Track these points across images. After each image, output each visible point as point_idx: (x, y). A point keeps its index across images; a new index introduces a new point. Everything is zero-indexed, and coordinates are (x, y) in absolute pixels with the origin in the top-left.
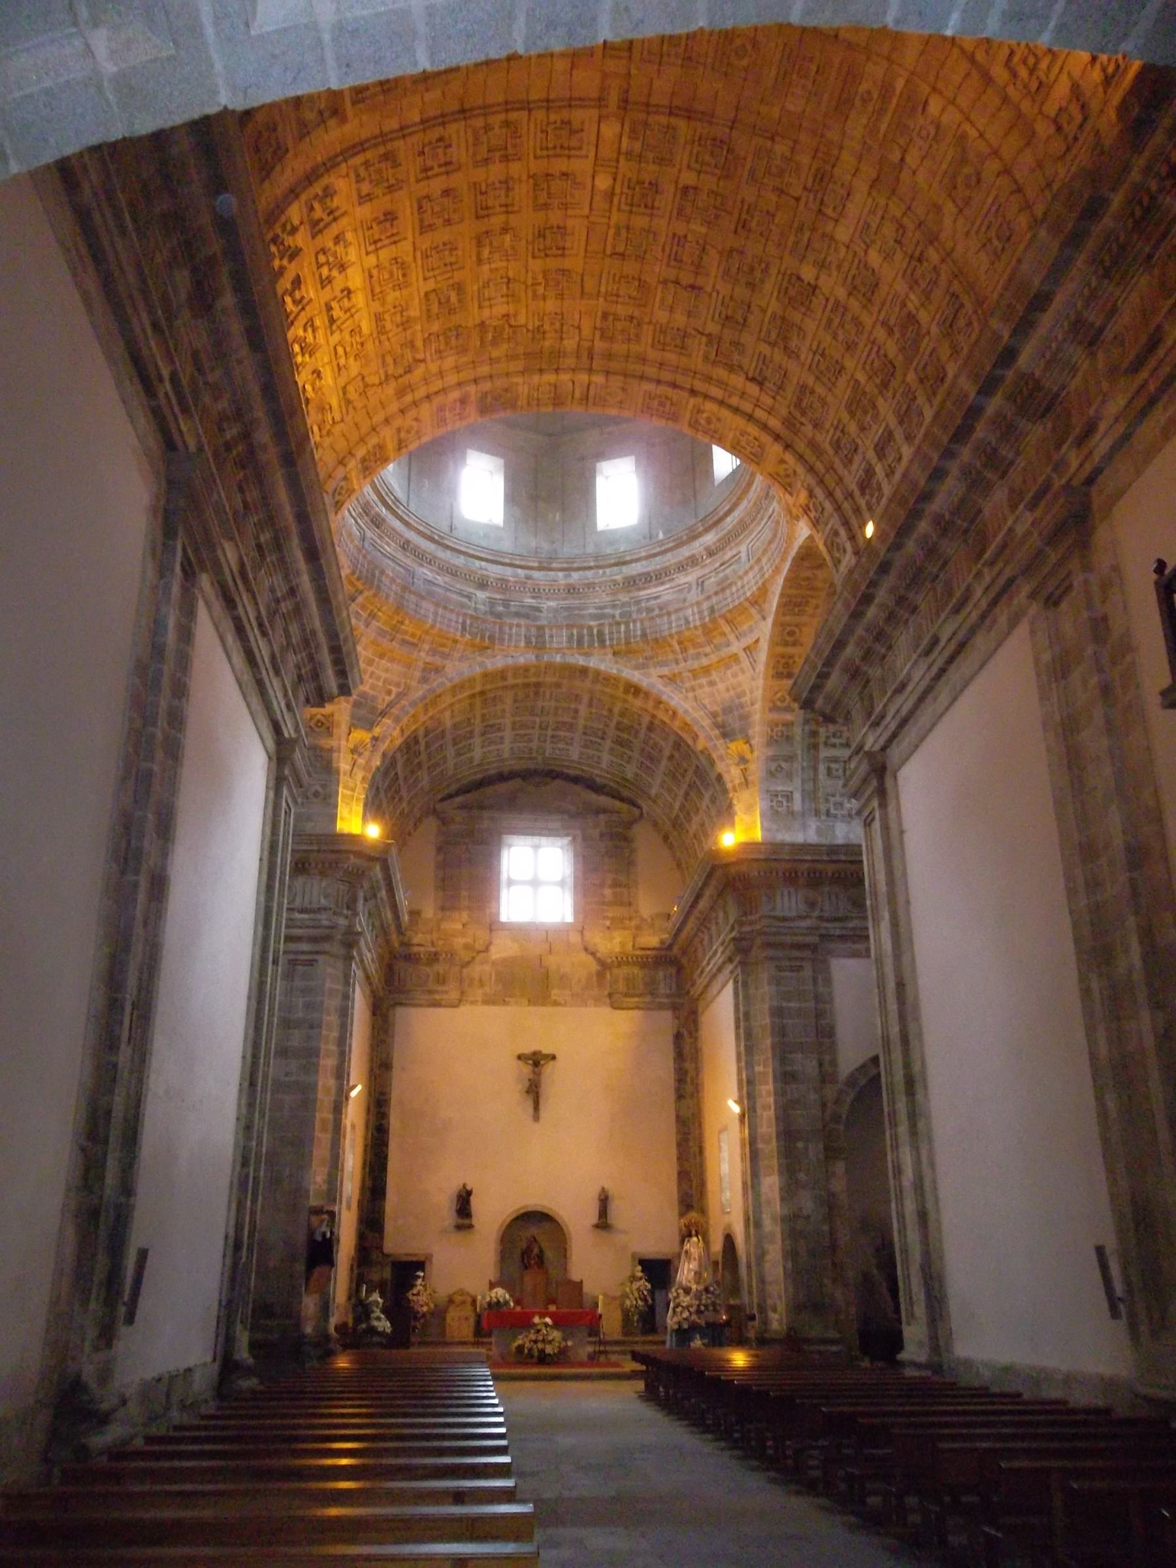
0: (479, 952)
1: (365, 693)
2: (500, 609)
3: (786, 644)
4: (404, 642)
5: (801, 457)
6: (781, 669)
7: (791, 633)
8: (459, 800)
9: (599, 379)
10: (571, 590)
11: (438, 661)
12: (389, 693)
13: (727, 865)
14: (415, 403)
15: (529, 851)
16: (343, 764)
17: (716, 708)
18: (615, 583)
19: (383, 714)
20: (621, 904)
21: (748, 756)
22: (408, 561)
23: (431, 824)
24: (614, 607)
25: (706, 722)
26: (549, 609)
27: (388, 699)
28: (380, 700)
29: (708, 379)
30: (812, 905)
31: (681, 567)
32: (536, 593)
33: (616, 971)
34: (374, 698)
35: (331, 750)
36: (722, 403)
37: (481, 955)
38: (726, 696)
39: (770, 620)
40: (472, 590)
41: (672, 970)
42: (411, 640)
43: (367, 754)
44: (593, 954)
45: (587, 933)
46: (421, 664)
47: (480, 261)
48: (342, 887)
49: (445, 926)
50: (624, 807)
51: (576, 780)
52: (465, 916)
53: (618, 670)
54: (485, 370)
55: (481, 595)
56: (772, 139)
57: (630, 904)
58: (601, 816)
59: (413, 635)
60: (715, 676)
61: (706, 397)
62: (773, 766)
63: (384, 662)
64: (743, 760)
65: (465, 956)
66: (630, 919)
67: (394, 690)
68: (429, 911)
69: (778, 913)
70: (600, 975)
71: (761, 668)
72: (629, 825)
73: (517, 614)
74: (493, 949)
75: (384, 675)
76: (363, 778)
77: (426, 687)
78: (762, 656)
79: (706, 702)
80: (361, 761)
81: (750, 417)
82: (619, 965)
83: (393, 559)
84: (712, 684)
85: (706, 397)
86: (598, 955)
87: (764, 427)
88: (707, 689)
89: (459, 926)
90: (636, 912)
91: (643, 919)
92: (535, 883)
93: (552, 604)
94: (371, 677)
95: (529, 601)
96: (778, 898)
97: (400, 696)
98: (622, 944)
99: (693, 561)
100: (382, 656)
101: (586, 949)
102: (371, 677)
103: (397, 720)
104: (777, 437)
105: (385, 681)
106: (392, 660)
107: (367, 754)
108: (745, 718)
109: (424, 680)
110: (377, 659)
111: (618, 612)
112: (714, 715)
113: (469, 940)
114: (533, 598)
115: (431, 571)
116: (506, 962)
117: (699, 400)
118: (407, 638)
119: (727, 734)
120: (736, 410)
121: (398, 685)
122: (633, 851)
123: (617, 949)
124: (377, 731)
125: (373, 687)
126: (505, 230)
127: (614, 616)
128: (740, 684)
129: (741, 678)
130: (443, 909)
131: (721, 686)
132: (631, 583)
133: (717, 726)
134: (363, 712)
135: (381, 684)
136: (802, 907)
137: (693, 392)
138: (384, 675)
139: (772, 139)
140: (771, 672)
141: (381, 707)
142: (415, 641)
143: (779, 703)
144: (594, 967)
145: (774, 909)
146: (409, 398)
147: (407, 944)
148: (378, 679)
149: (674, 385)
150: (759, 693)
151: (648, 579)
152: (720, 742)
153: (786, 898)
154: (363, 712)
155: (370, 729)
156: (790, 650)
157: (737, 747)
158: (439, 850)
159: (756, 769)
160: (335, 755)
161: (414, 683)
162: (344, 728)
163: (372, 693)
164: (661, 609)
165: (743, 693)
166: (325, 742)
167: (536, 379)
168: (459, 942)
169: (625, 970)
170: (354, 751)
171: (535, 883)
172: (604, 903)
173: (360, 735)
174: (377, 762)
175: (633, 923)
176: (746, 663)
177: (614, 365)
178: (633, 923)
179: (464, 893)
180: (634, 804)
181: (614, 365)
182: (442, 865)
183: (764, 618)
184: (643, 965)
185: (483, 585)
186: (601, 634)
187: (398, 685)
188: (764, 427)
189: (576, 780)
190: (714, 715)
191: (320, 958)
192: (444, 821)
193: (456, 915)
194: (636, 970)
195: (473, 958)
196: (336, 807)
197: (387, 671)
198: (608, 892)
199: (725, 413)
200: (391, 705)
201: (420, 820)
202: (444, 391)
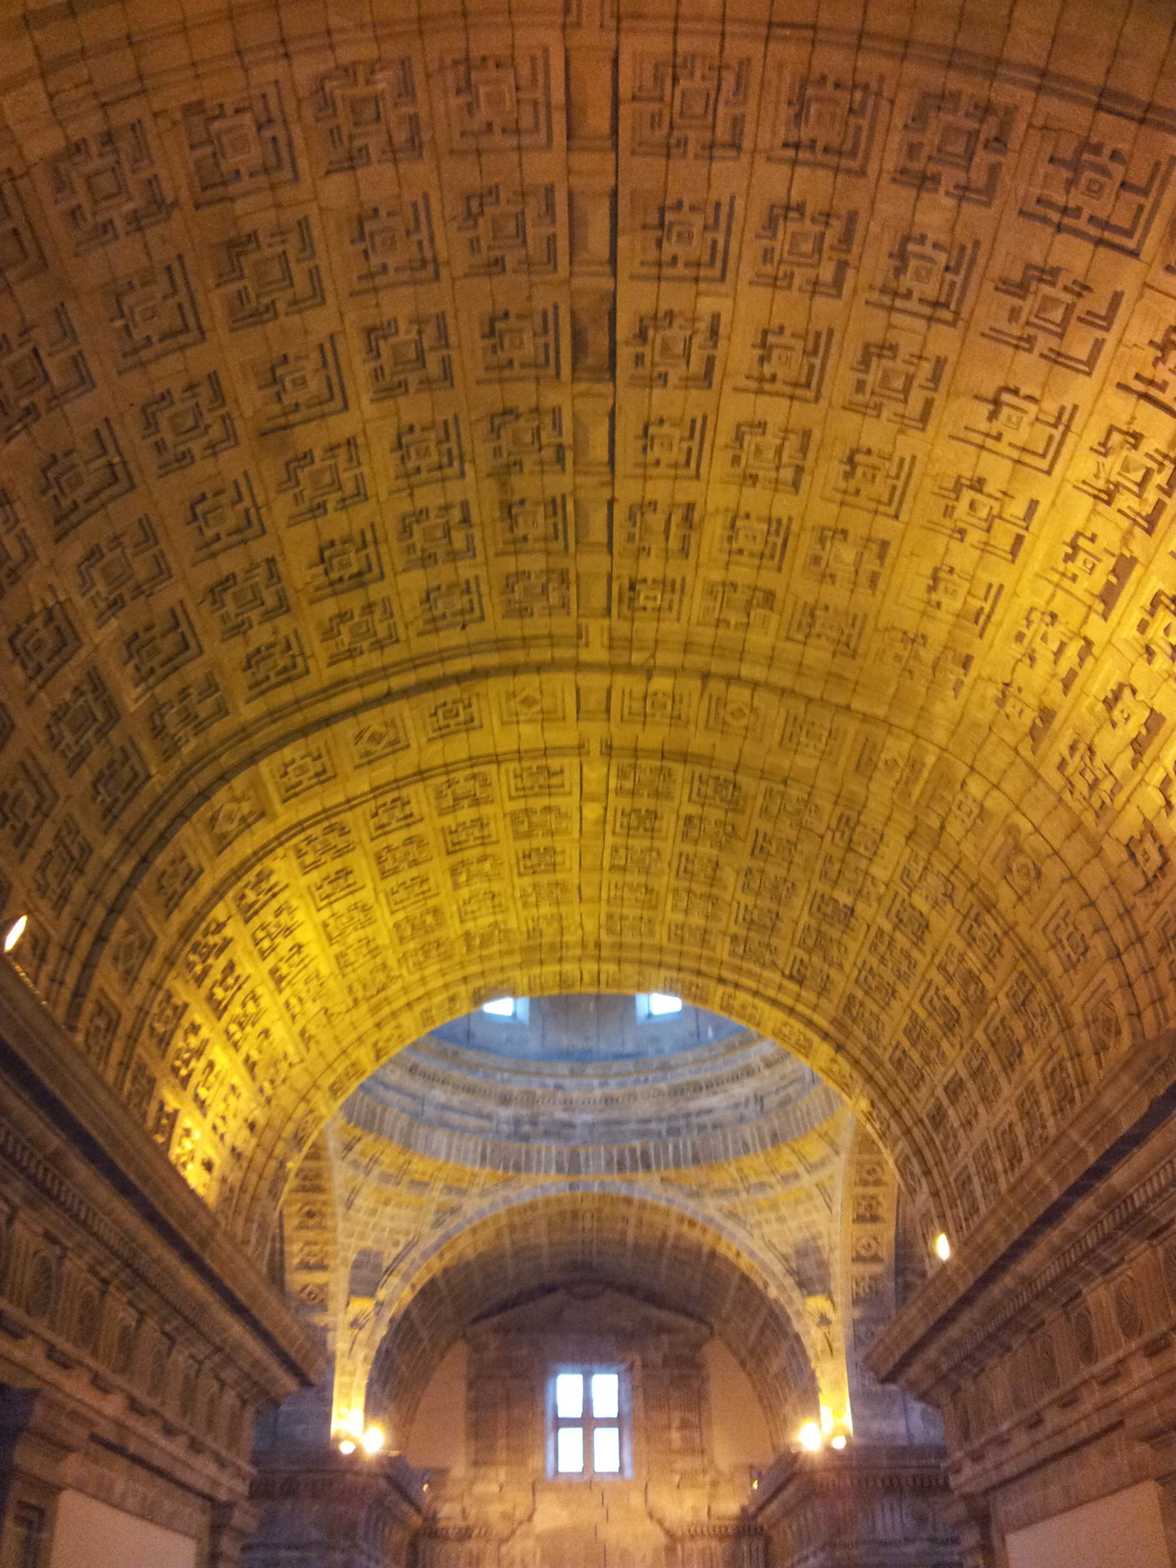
0: (520, 1523)
2: (526, 1128)
3: (865, 1183)
4: (413, 1183)
5: (856, 1063)
6: (862, 1211)
7: (871, 1172)
8: (495, 1320)
9: (610, 968)
10: (609, 1100)
11: (454, 1200)
12: (396, 1244)
13: (813, 1472)
14: (394, 1015)
15: (579, 1378)
16: (340, 1343)
17: (787, 1250)
18: (660, 1093)
19: (390, 1271)
20: (693, 1451)
21: (832, 1316)
22: (415, 1085)
23: (460, 1349)
24: (660, 1120)
25: (778, 1268)
26: (584, 1124)
27: (395, 1252)
29: (739, 970)
30: (921, 1520)
31: (735, 1078)
32: (568, 1105)
33: (689, 1545)
34: (379, 1254)
35: (325, 1329)
36: (756, 993)
37: (524, 1528)
38: (800, 1236)
39: (843, 1156)
41: (761, 1544)
43: (369, 1326)
44: (660, 1522)
45: (652, 1497)
46: (434, 1207)
47: (456, 886)
49: (480, 1488)
50: (691, 1324)
51: (631, 1290)
52: (502, 1474)
53: (669, 1201)
54: (474, 968)
55: (505, 1113)
56: (785, 782)
57: (703, 1452)
58: (664, 1337)
60: (784, 1211)
61: (737, 986)
62: (862, 1329)
63: (389, 1210)
64: (824, 1321)
65: (502, 1528)
66: (704, 1471)
67: (403, 1241)
68: (459, 1469)
69: (881, 1535)
70: (670, 1550)
71: (837, 1209)
72: (698, 1346)
73: (547, 1134)
74: (537, 1518)
75: (389, 1224)
76: (366, 1358)
77: (440, 1232)
78: (839, 1195)
79: (775, 1240)
80: (363, 1335)
81: (791, 1011)
82: (693, 1537)
83: (399, 1089)
84: (781, 1219)
85: (737, 986)
86: (667, 1524)
87: (810, 1023)
88: (775, 1226)
89: (495, 1488)
90: (711, 1461)
91: (719, 1473)
92: (587, 1422)
93: (588, 1117)
95: (560, 1115)
96: (878, 1512)
97: (410, 1246)
98: (695, 1510)
99: (749, 1072)
100: (386, 1203)
101: (651, 1516)
103: (406, 1277)
104: (826, 1036)
106: (399, 1205)
107: (369, 1326)
108: (823, 1265)
109: (437, 1224)
111: (664, 1127)
112: (785, 1258)
113: (508, 1507)
116: (555, 1537)
117: (730, 990)
119: (806, 1285)
120: (774, 1002)
122: (704, 1380)
123: (689, 1518)
124: (382, 1294)
126: (483, 859)
127: (659, 1134)
128: (814, 1222)
129: (815, 1216)
130: (476, 1464)
131: (793, 1224)
132: (677, 1092)
133: (791, 1272)
134: (364, 1273)
136: (909, 1522)
137: (721, 980)
139: (785, 782)
140: (851, 1216)
141: (386, 1264)
143: (863, 1252)
144: (662, 1539)
145: (873, 1529)
146: (386, 1011)
147: (431, 1519)
149: (699, 973)
150: (837, 1239)
151: (696, 1088)
152: (796, 1294)
153: (888, 1513)
154: (364, 1273)
155: (371, 1294)
156: (871, 1190)
157: (817, 1303)
158: (471, 1385)
159: (840, 1333)
160: (330, 1335)
161: (426, 1230)
162: (341, 1298)
163: (376, 1248)
164: (715, 1127)
165: (820, 1235)
166: (319, 1319)
167: (536, 971)
168: (494, 1511)
169: (700, 1544)
170: (355, 1324)
171: (587, 1422)
172: (672, 1452)
173: (362, 1305)
174: (383, 1331)
175: (708, 1478)
176: (820, 1201)
177: (628, 954)
178: (708, 1478)
179: (501, 1443)
180: (701, 1320)
181: (628, 954)
182: (473, 1406)
183: (837, 1153)
184: (721, 1536)
185: (505, 1100)
186: (645, 1154)
187: (407, 1233)
188: (810, 1023)
189: (631, 1290)
190: (785, 1258)
192: (477, 1348)
193: (492, 1473)
194: (714, 1544)
195: (513, 1532)
196: (329, 1402)
197: (392, 1218)
198: (675, 1436)
199: (759, 1003)
200: (399, 1259)
201: (448, 1347)
202: (428, 995)
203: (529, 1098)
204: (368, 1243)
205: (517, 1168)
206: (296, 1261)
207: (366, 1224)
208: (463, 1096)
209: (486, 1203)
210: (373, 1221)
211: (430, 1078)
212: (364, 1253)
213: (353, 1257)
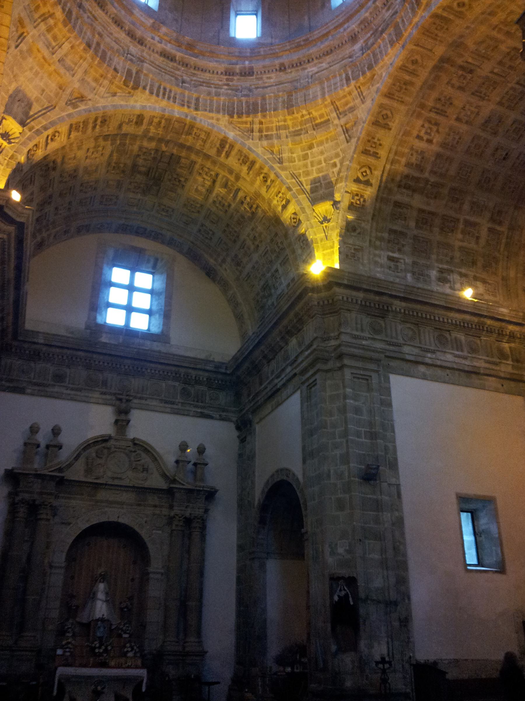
1: (315, 179)
12: (335, 165)
27: (336, 170)
28: (331, 175)
34: (325, 177)
40: (350, 50)
42: (322, 120)
48: (332, 318)
59: (321, 116)
63: (315, 150)
67: (337, 160)
75: (322, 158)
94: (312, 166)
100: (311, 147)
102: (312, 166)
105: (325, 161)
106: (321, 143)
110: (309, 152)
114: (388, 10)
115: (315, 65)
118: (319, 121)
121: (337, 155)
125: (319, 171)
135: (324, 164)
138: (322, 158)
142: (326, 118)
148: (320, 163)
161: (345, 145)
163: (320, 175)
185: (354, 38)
191: (317, 376)
197: (322, 153)
203: (365, 24)
204: (315, 175)
205: (370, 67)
206: (280, 209)
207: (306, 166)
208: (328, 59)
209: (368, 103)
210: (309, 161)
211: (299, 64)
212: (315, 181)
213: (308, 188)
